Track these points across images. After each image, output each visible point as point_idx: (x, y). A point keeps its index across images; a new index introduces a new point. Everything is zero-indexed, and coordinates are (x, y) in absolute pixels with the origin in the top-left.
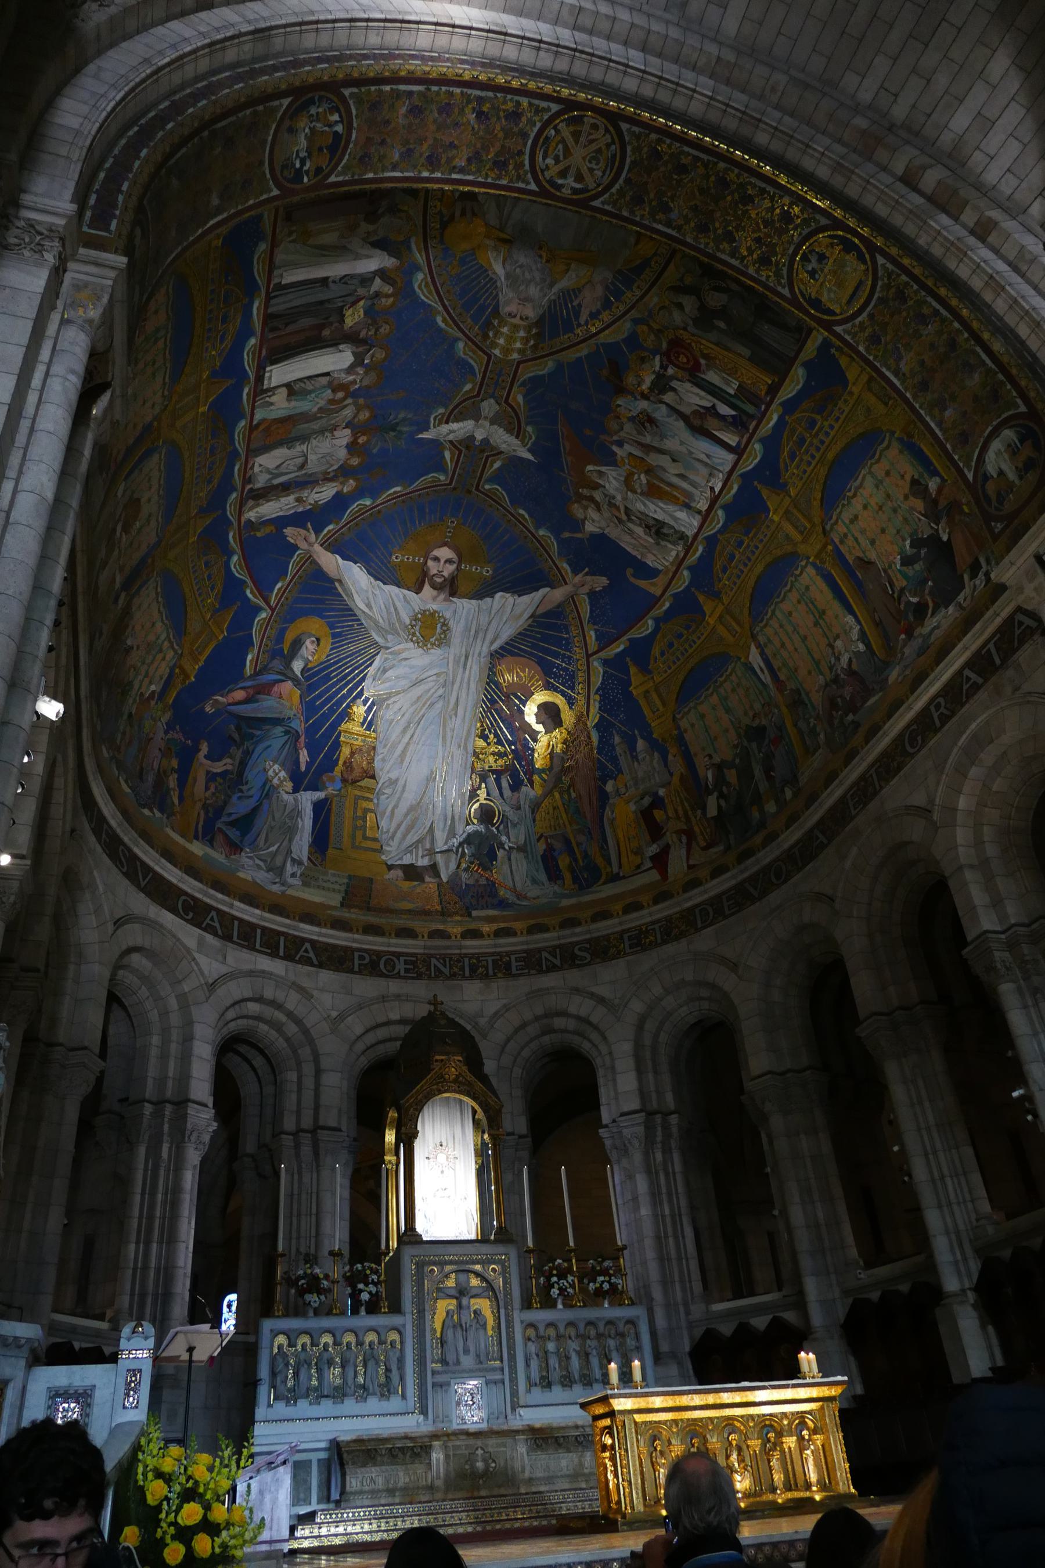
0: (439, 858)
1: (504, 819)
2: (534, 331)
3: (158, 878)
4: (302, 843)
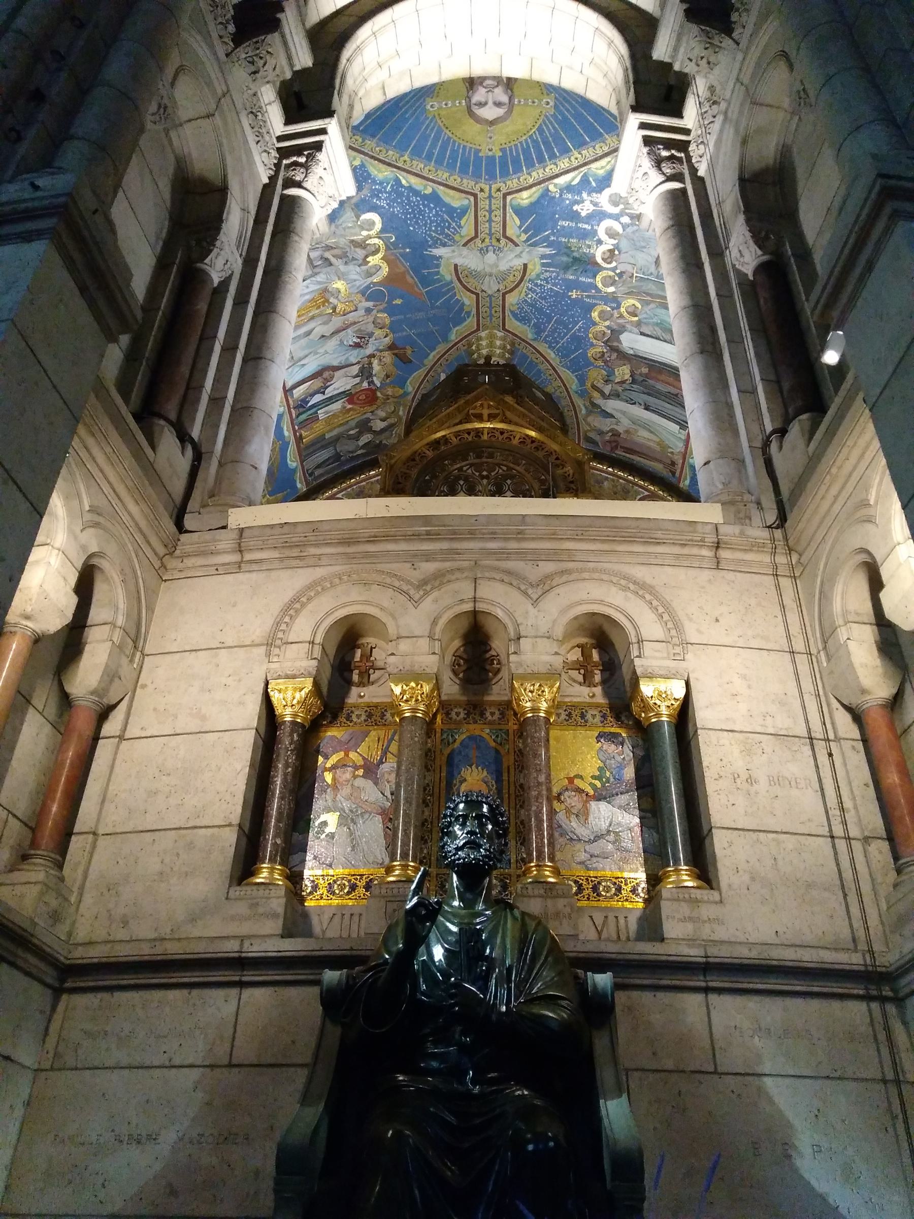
2: (475, 356)
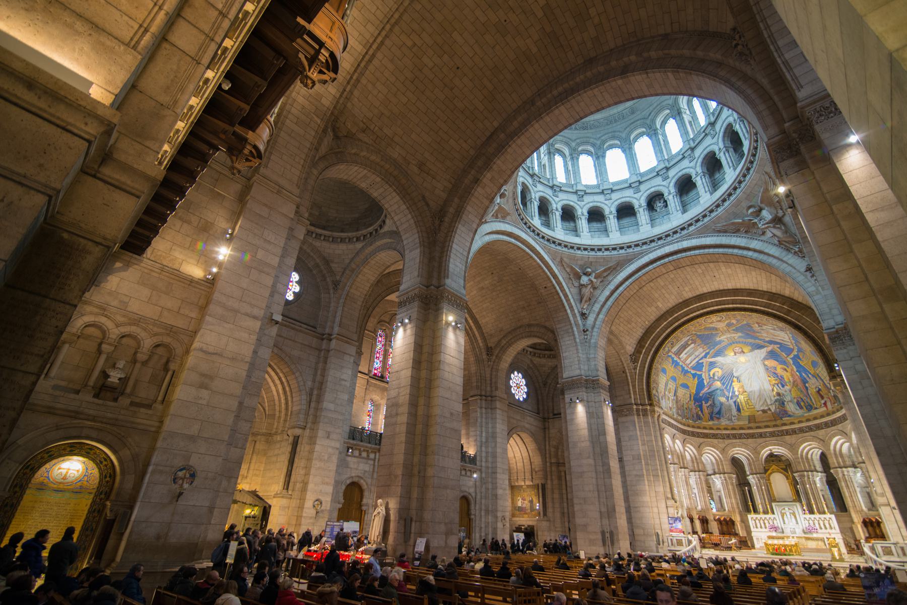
0: (770, 407)
1: (783, 395)
3: (704, 433)
4: (734, 412)
